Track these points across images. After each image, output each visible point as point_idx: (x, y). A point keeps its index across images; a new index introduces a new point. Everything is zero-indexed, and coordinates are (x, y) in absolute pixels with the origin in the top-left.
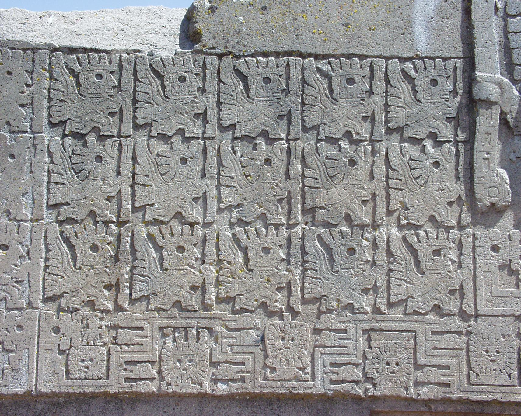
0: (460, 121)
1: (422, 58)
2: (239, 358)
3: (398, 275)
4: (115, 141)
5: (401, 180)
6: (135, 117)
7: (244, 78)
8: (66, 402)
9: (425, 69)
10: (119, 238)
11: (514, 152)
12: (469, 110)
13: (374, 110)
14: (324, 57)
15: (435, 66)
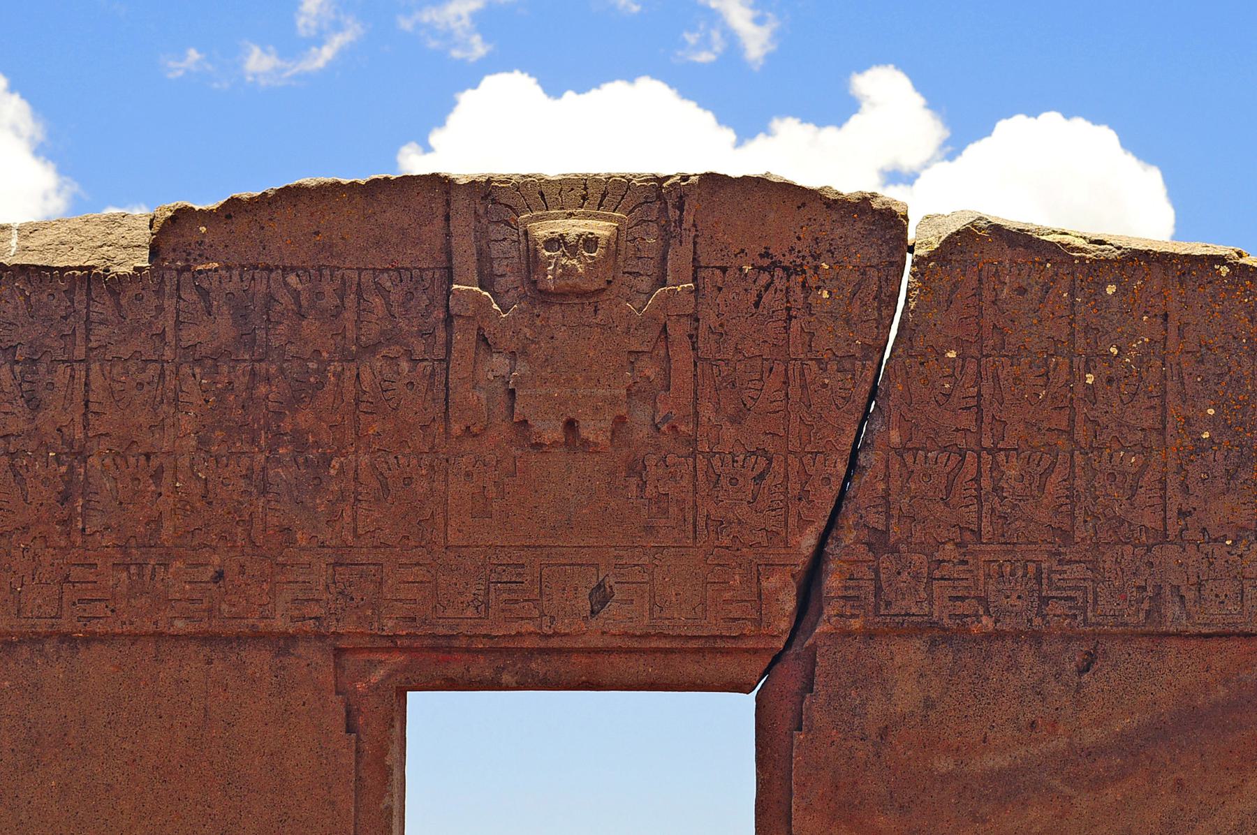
0: (437, 338)
1: (398, 270)
2: (196, 595)
3: (364, 505)
4: (67, 366)
5: (372, 403)
6: (88, 340)
7: (204, 294)
8: (19, 641)
9: (401, 281)
10: (71, 469)
11: (493, 371)
12: (446, 326)
13: (345, 327)
14: (293, 269)
15: (411, 277)
